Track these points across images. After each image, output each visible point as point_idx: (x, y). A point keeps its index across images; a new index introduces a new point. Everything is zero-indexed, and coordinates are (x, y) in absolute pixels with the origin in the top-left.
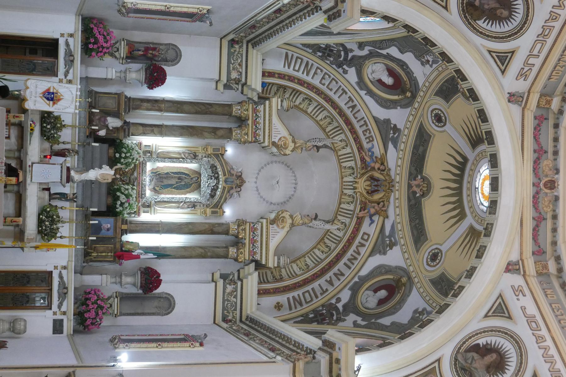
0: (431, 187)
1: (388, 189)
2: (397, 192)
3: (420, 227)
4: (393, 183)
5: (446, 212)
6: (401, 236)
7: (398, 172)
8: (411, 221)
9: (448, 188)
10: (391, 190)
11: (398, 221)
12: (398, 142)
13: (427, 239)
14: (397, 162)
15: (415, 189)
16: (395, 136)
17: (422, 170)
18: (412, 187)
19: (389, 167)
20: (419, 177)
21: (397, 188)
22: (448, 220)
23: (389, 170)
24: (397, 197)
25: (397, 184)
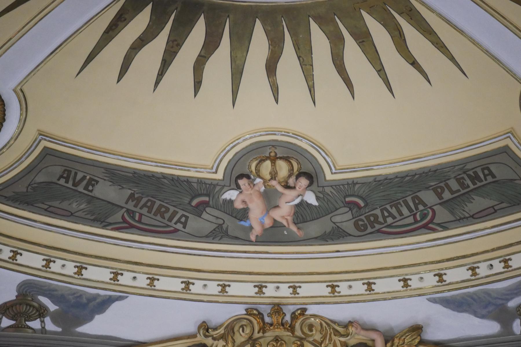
0: (274, 144)
1: (292, 329)
2: (305, 290)
3: (454, 185)
4: (266, 310)
5: (381, 71)
6: (498, 267)
7: (213, 288)
8: (427, 224)
9: (271, 68)
10: (294, 317)
11: (431, 280)
12: (79, 295)
13: (506, 150)
14: (167, 295)
15: (284, 212)
16: (52, 307)
17: (201, 181)
18: (276, 225)
19: (192, 328)
20: (231, 195)
21: (285, 291)
22: (414, 63)
23: (205, 328)
24: (323, 290)
25: (270, 291)
